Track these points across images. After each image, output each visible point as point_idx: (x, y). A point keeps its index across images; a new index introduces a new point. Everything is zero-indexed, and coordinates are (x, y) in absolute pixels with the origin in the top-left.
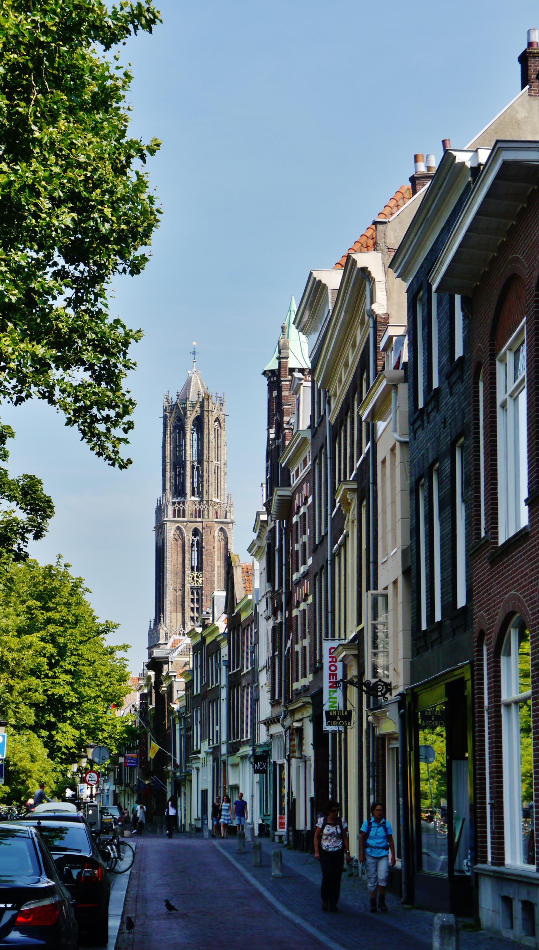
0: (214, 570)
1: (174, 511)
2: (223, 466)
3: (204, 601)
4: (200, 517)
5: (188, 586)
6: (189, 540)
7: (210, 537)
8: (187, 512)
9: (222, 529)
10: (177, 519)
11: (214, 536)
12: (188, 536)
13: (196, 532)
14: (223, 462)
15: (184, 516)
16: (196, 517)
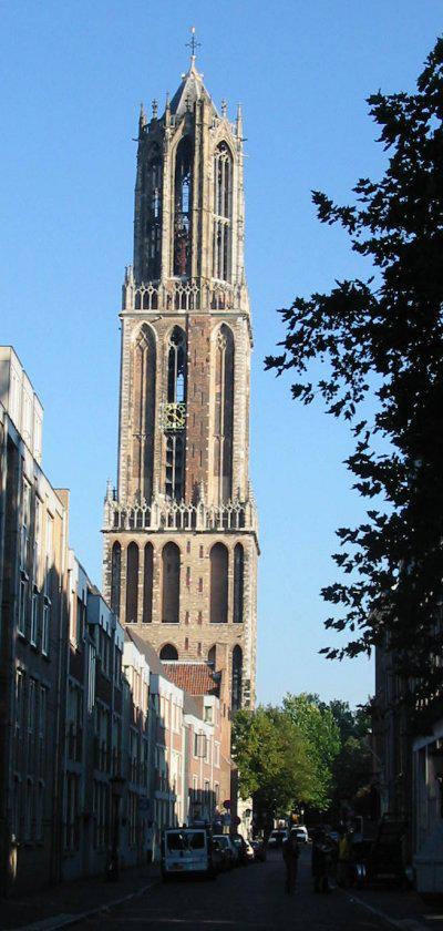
0: (208, 400)
1: (138, 297)
2: (235, 226)
3: (189, 455)
4: (184, 307)
5: (160, 428)
6: (163, 348)
7: (203, 340)
8: (160, 298)
9: (224, 328)
10: (142, 311)
11: (208, 339)
12: (164, 342)
13: (178, 336)
14: (235, 217)
15: (155, 306)
16: (177, 308)
